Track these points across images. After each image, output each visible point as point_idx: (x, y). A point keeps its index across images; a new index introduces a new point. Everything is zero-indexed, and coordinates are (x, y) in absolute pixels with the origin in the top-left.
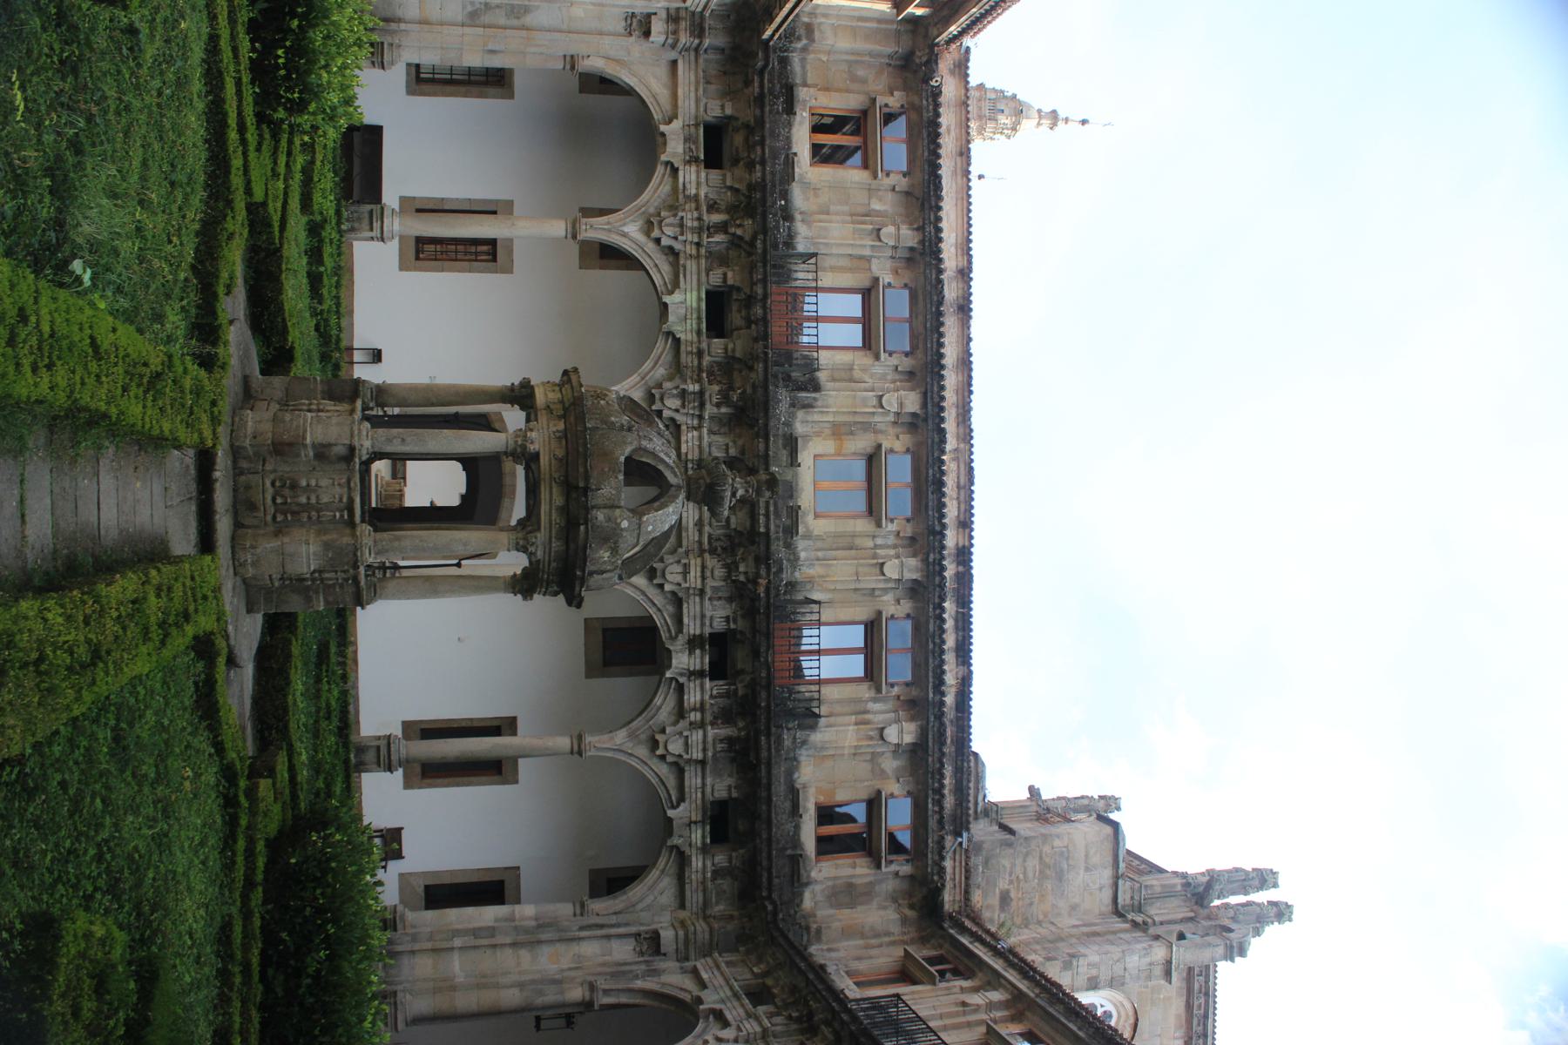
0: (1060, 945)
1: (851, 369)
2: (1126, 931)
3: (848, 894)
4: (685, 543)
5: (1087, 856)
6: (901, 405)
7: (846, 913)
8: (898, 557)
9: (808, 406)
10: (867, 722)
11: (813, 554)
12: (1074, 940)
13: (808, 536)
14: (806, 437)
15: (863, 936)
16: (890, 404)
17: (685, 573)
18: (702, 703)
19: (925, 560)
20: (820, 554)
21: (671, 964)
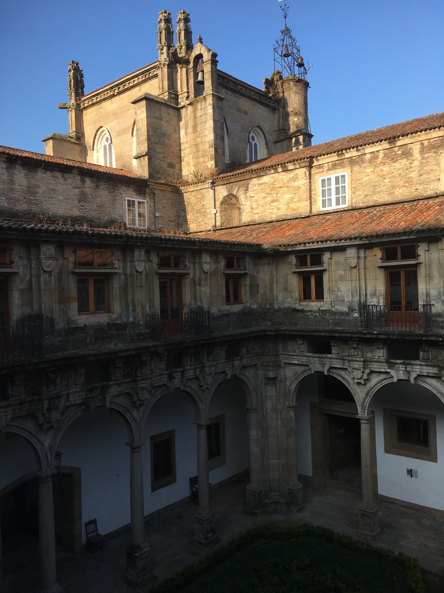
0: (201, 148)
1: (22, 291)
2: (195, 111)
3: (254, 287)
4: (127, 391)
5: (156, 118)
6: (50, 258)
7: (261, 291)
8: (132, 261)
9: (52, 322)
10: (200, 279)
11: (131, 314)
12: (199, 140)
13: (120, 317)
14: (68, 321)
15: (272, 284)
16: (49, 266)
17: (143, 389)
18: (193, 369)
19: (138, 247)
20: (130, 309)
21: (282, 372)
